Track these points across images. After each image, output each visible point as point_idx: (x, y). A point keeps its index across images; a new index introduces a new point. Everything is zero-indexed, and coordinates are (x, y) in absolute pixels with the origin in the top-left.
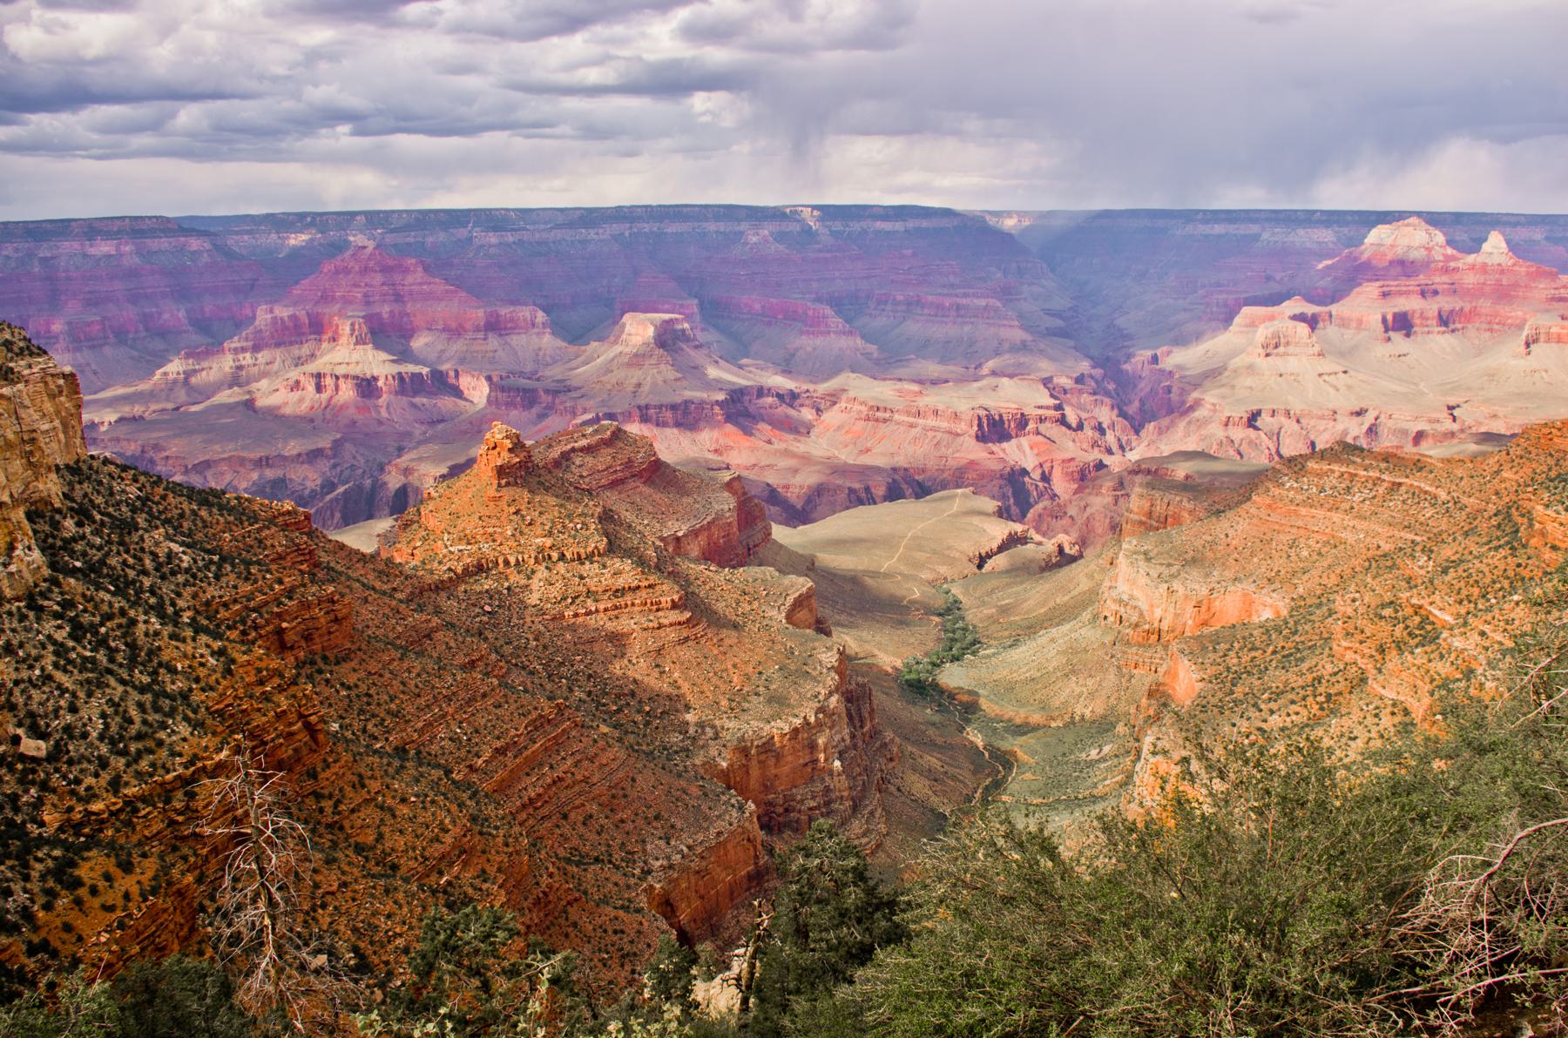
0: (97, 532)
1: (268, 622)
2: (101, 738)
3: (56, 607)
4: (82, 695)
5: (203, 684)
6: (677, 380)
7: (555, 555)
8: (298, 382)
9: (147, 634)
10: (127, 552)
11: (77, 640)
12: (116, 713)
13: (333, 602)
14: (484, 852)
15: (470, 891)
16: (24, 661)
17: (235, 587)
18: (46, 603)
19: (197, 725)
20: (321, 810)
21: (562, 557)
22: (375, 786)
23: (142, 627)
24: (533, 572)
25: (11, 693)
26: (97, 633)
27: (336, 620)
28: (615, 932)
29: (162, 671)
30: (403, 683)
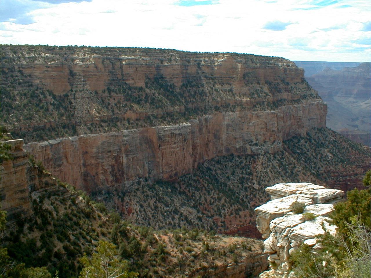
3: (279, 158)
10: (315, 152)
23: (297, 168)
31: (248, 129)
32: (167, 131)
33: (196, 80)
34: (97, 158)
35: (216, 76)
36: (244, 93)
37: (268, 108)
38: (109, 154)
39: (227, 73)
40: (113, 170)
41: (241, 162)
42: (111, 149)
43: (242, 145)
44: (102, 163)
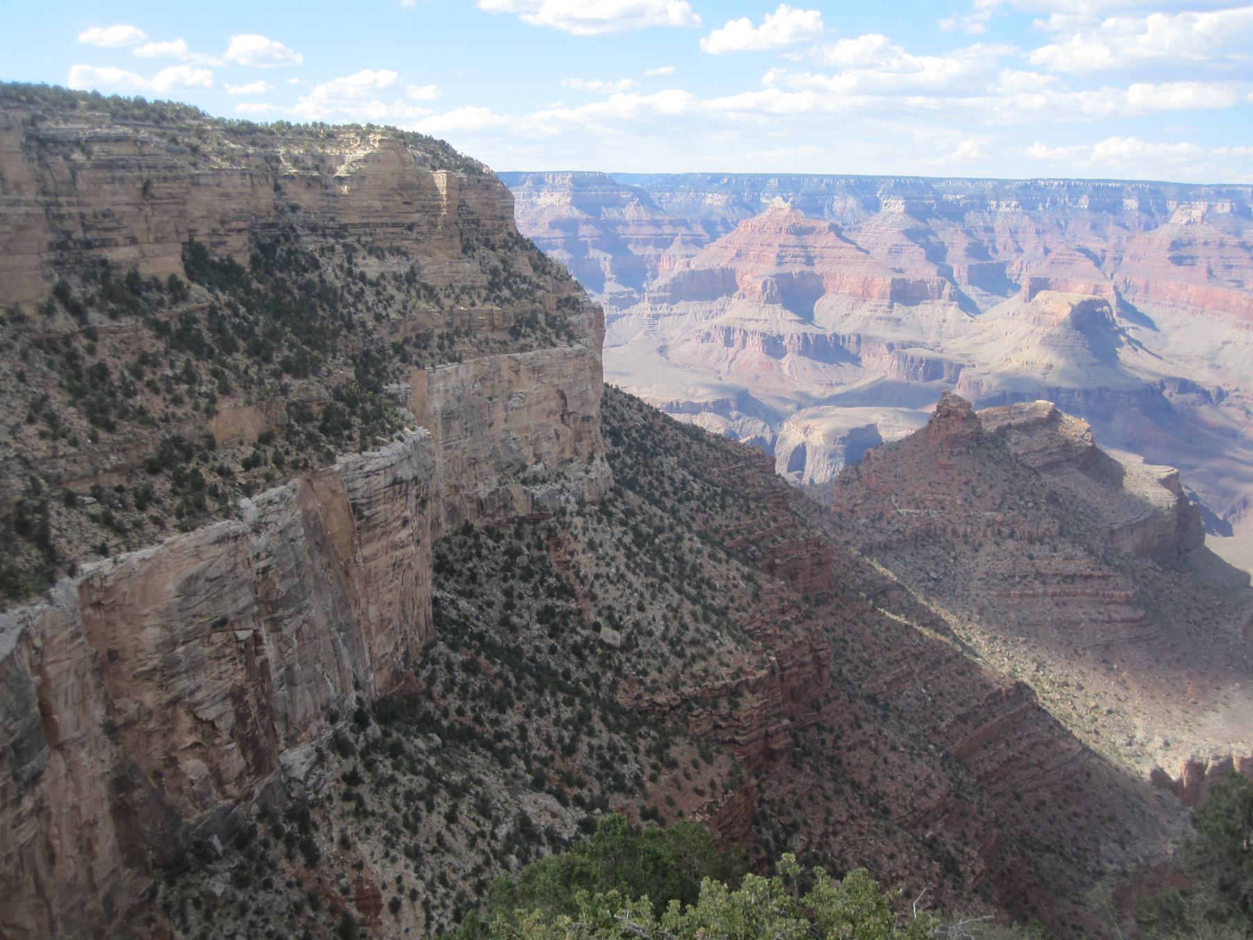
0: (627, 452)
1: (764, 557)
2: (664, 638)
3: (621, 515)
4: (647, 596)
5: (736, 605)
6: (1092, 365)
7: (1006, 530)
8: (708, 335)
9: (691, 551)
10: (651, 473)
11: (639, 546)
12: (675, 617)
13: (819, 546)
14: (962, 815)
15: (953, 851)
16: (603, 558)
17: (738, 519)
18: (614, 510)
19: (740, 642)
20: (823, 742)
21: (1012, 535)
22: (867, 728)
24: (980, 544)
25: (592, 586)
26: (652, 543)
27: (819, 564)
28: (1074, 927)
29: (704, 586)
30: (875, 635)
31: (506, 421)
32: (375, 472)
33: (282, 239)
34: (166, 672)
35: (345, 221)
36: (469, 284)
37: (558, 336)
38: (219, 638)
39: (385, 208)
40: (241, 718)
41: (513, 553)
42: (229, 608)
43: (494, 486)
44: (192, 693)
